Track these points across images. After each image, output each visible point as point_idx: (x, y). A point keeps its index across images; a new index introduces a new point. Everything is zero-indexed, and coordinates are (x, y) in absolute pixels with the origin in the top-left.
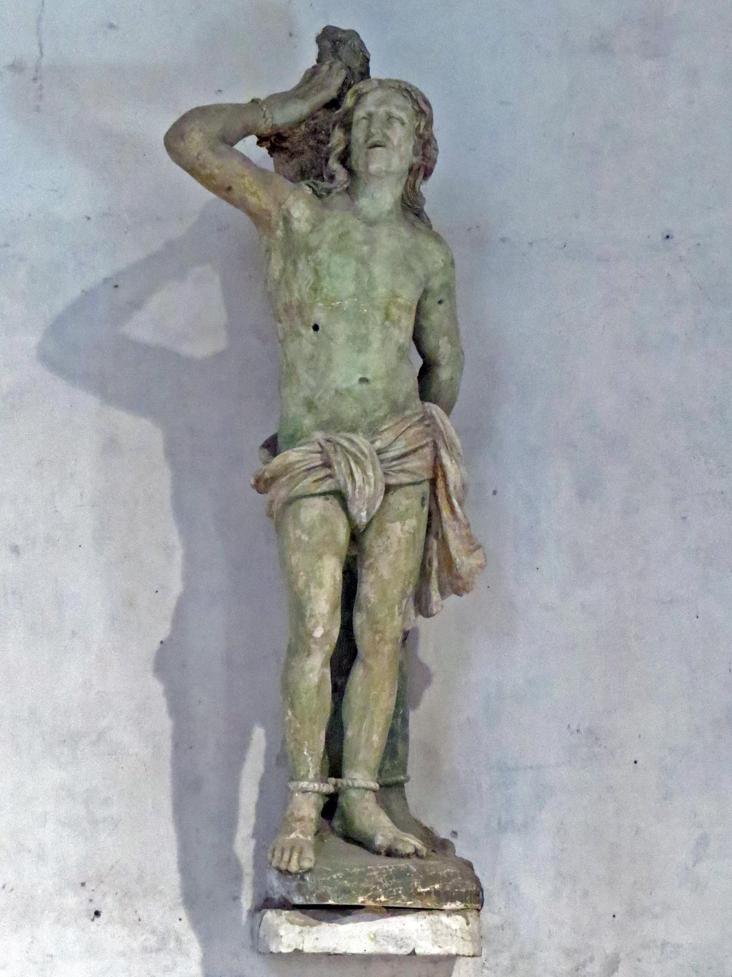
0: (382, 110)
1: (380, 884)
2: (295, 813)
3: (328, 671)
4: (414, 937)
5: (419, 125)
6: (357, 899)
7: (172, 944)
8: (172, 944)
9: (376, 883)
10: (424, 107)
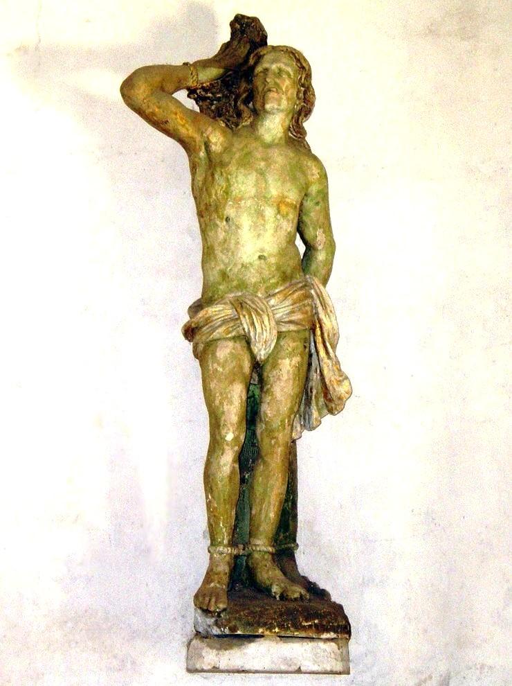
0: (274, 67)
1: (275, 619)
2: (214, 568)
3: (237, 466)
4: (300, 658)
5: (301, 78)
6: (257, 632)
7: (129, 665)
8: (129, 665)
9: (272, 619)
10: (304, 65)
